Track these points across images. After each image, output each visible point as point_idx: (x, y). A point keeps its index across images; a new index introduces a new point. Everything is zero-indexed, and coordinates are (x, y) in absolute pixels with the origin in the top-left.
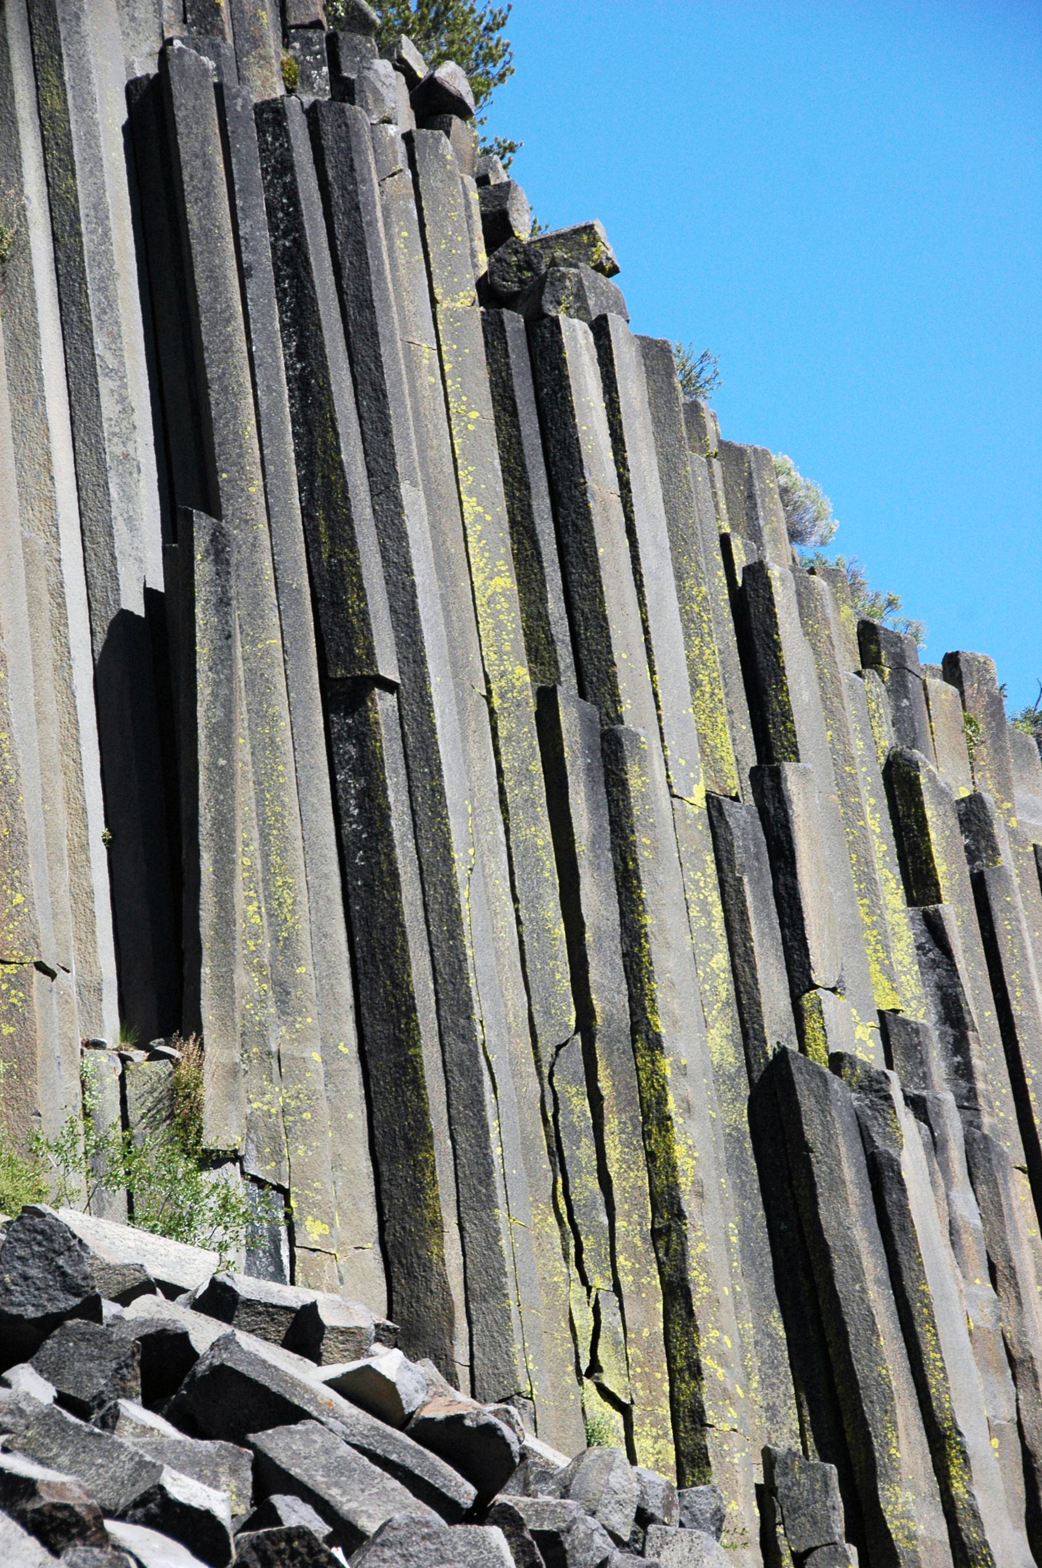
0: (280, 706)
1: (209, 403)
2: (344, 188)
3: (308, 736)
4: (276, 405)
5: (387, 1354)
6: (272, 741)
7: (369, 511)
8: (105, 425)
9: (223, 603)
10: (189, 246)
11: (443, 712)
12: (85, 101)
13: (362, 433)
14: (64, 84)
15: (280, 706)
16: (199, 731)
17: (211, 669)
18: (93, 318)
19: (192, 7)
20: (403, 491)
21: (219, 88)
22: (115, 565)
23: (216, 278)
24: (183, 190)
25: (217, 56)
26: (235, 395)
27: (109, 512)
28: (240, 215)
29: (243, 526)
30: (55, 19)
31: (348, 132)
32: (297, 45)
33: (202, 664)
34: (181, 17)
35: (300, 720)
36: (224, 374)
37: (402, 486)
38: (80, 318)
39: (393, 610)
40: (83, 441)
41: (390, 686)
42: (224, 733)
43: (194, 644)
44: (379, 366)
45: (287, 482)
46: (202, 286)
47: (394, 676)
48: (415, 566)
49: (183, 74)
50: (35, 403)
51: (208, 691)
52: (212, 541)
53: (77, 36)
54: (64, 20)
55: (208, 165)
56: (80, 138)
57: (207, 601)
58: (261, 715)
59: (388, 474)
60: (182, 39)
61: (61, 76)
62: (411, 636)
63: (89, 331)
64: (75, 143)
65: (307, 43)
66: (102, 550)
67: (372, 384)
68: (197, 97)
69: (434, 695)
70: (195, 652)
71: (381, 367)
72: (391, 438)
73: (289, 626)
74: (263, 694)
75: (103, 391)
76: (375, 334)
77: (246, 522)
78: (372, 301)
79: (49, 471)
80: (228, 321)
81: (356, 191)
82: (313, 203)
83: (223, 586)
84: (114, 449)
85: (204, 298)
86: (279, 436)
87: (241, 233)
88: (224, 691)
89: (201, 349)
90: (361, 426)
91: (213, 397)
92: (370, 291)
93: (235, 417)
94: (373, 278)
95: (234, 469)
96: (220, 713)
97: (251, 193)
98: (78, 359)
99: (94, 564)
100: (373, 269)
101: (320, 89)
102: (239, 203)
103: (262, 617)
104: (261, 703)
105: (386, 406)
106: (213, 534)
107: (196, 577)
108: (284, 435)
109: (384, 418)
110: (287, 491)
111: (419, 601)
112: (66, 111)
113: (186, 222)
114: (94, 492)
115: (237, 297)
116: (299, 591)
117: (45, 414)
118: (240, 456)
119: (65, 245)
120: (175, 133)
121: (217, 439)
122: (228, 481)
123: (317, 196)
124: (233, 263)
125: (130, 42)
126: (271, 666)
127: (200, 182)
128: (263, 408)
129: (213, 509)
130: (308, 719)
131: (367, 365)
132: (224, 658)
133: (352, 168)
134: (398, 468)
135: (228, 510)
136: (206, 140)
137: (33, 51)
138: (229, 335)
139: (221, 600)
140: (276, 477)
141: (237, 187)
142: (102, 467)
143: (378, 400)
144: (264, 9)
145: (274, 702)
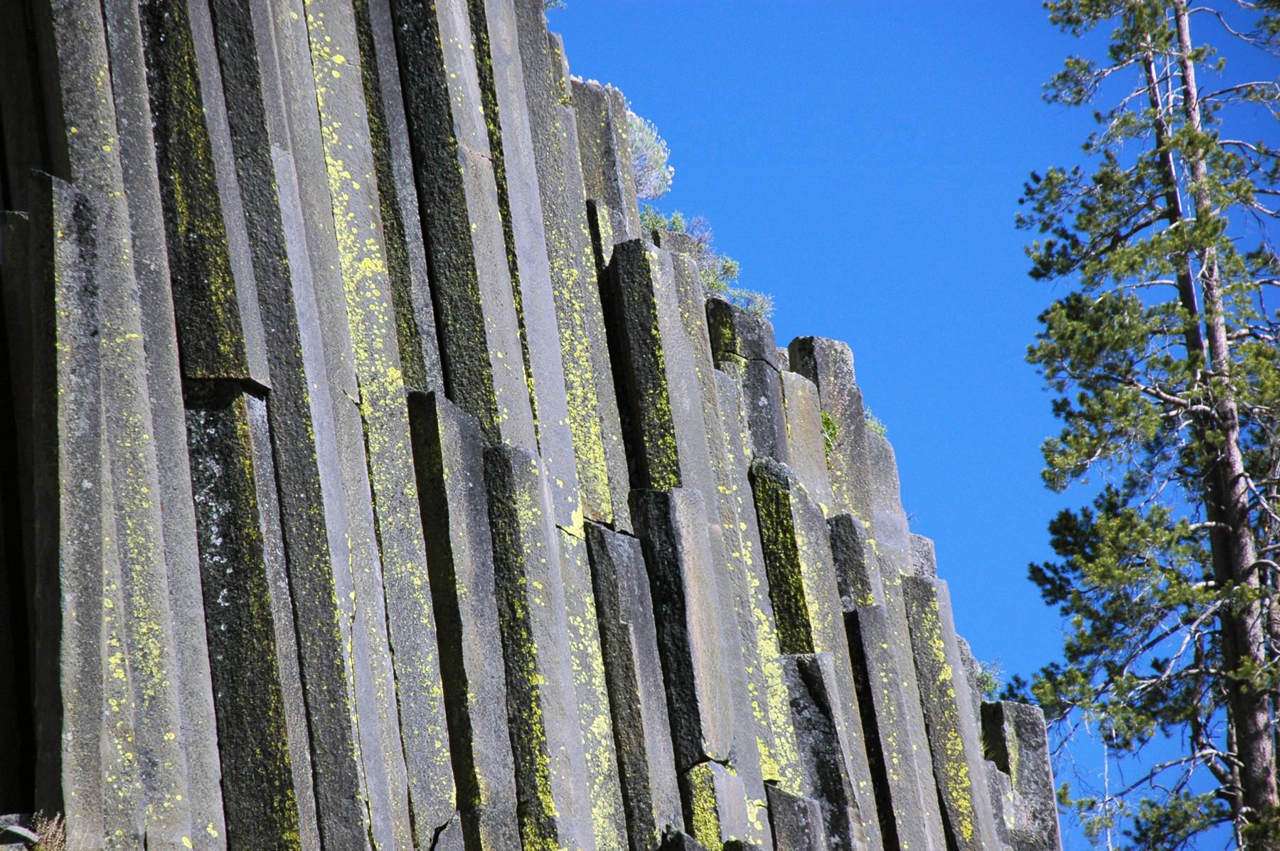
7: (233, 177)
9: (88, 291)
20: (273, 154)
26: (85, 31)
39: (262, 300)
47: (264, 381)
52: (74, 215)
70: (55, 350)
77: (101, 188)
83: (88, 272)
90: (222, 72)
91: (59, 32)
93: (85, 58)
95: (85, 122)
96: (84, 424)
103: (121, 306)
105: (253, 51)
106: (76, 208)
111: (294, 290)
116: (158, 273)
118: (92, 106)
122: (79, 137)
126: (132, 365)
134: (268, 128)
139: (86, 290)
143: (242, 42)
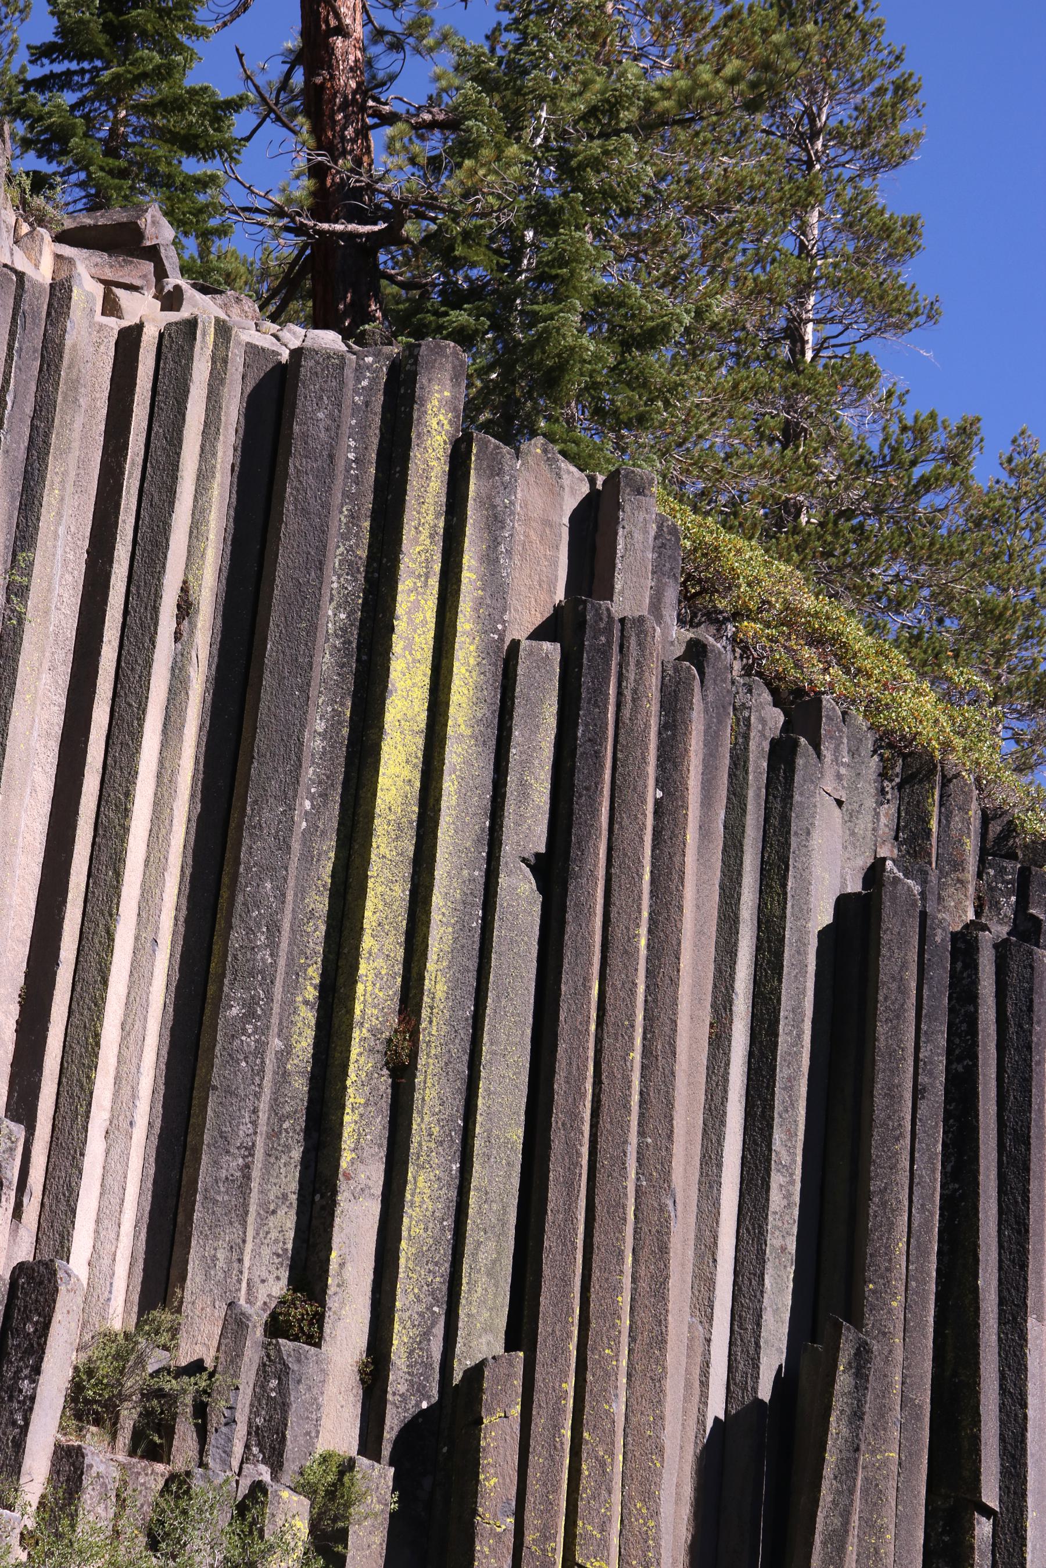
0: (888, 1520)
1: (868, 1214)
2: (1020, 1026)
3: (908, 1551)
4: (927, 1223)
5: (9, 1258)
6: (877, 1551)
7: (995, 1338)
8: (770, 1218)
9: (857, 1416)
10: (874, 1062)
11: (1034, 1547)
12: (801, 910)
13: (1000, 1261)
14: (785, 893)
15: (888, 1520)
16: (817, 1536)
17: (836, 1478)
18: (776, 1115)
19: (905, 827)
20: (1029, 1324)
21: (923, 915)
22: (758, 1354)
23: (893, 1095)
24: (876, 1008)
25: (924, 882)
26: (893, 1211)
27: (761, 1302)
28: (923, 1039)
29: (880, 1337)
30: (788, 832)
31: (1032, 974)
32: (992, 872)
33: (828, 1472)
34: (893, 834)
35: (903, 1532)
36: (886, 1189)
37: (1029, 1320)
38: (763, 1112)
39: (1002, 1439)
40: (747, 1229)
41: (988, 1512)
42: (838, 1540)
43: (825, 1450)
44: (1026, 1201)
45: (925, 1300)
46: (879, 1101)
47: (993, 1503)
48: (1030, 1400)
49: (894, 898)
50: (711, 1187)
51: (830, 1498)
52: (855, 1354)
53: (804, 850)
54: (796, 833)
55: (903, 990)
56: (791, 944)
57: (842, 1411)
58: (870, 1525)
59: (1017, 1306)
60: (893, 861)
61: (784, 886)
62: (1015, 1468)
63: (771, 1127)
64: (786, 949)
65: (1001, 871)
66: (748, 1336)
67: (1015, 1217)
68: (903, 924)
69: (1029, 1529)
70: (824, 1459)
71: (1028, 1202)
72: (1026, 1272)
73: (907, 1439)
74: (875, 1504)
75: (774, 1186)
76: (1027, 1170)
77: (884, 1334)
78: (1029, 1137)
79: (714, 1254)
80: (897, 1139)
81: (1031, 1032)
82: (989, 1035)
83: (859, 1401)
84: (774, 1242)
85: (879, 1115)
86: (924, 1253)
87: (921, 1056)
88: (843, 1501)
89: (869, 1161)
90: (1000, 1254)
91: (873, 1208)
92: (1029, 1128)
93: (889, 1232)
94: (1033, 1116)
95: (881, 1281)
96: (837, 1522)
97: (936, 1019)
98: (756, 1151)
99: (739, 1349)
100: (1035, 1107)
101: (1006, 916)
102: (924, 1027)
103: (885, 1429)
104: (871, 1514)
105: (1027, 1240)
106: (858, 1349)
107: (837, 1387)
108: (929, 1254)
109: (1024, 1252)
110: (924, 1308)
111: (1029, 1435)
112: (783, 917)
113: (875, 1039)
114: (750, 1280)
115: (909, 1117)
116: (920, 1407)
117: (718, 1199)
118: (888, 1270)
119: (761, 1042)
120: (878, 953)
121: (869, 1250)
122: (874, 1292)
123: (993, 1029)
124: (909, 1085)
125: (847, 855)
126: (886, 1477)
127: (893, 1003)
128: (915, 1224)
129: (858, 1323)
130: (910, 1534)
131: (1015, 1198)
132: (848, 1469)
133: (1030, 1009)
134: (1029, 1302)
135: (869, 1321)
136: (904, 966)
137: (763, 857)
138: (897, 1153)
139: (855, 1414)
140: (917, 1293)
141: (924, 1012)
142: (761, 1258)
143: (1019, 1232)
144: (969, 837)
145: (883, 1514)
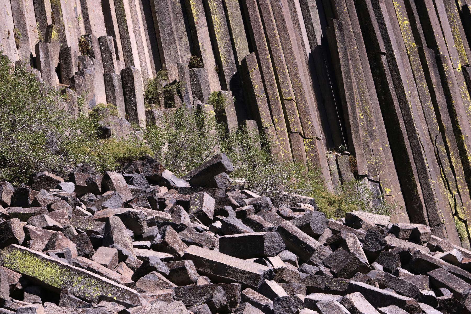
6: (359, 72)
7: (373, 11)
9: (343, 41)
11: (398, 58)
15: (360, 64)
17: (343, 58)
20: (380, 4)
22: (315, 34)
27: (311, 21)
29: (344, 20)
33: (340, 57)
35: (364, 66)
39: (382, 35)
41: (383, 54)
42: (348, 73)
43: (338, 52)
45: (352, 7)
47: (385, 51)
58: (355, 67)
66: (311, 31)
70: (338, 54)
73: (358, 43)
77: (345, 19)
79: (296, 13)
83: (343, 37)
84: (310, 5)
96: (346, 68)
103: (352, 42)
104: (355, 64)
106: (339, 24)
107: (336, 35)
111: (388, 31)
116: (359, 34)
122: (339, 9)
126: (356, 54)
129: (337, 18)
130: (366, 65)
132: (345, 54)
135: (340, 16)
142: (308, 10)
